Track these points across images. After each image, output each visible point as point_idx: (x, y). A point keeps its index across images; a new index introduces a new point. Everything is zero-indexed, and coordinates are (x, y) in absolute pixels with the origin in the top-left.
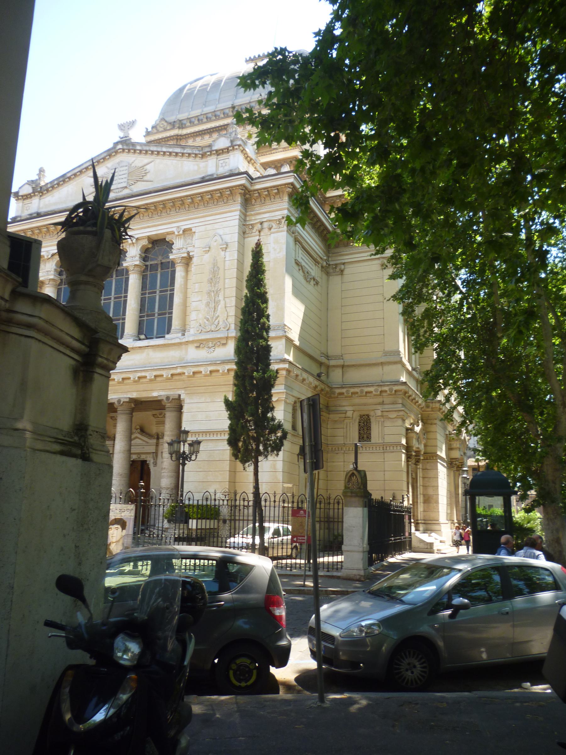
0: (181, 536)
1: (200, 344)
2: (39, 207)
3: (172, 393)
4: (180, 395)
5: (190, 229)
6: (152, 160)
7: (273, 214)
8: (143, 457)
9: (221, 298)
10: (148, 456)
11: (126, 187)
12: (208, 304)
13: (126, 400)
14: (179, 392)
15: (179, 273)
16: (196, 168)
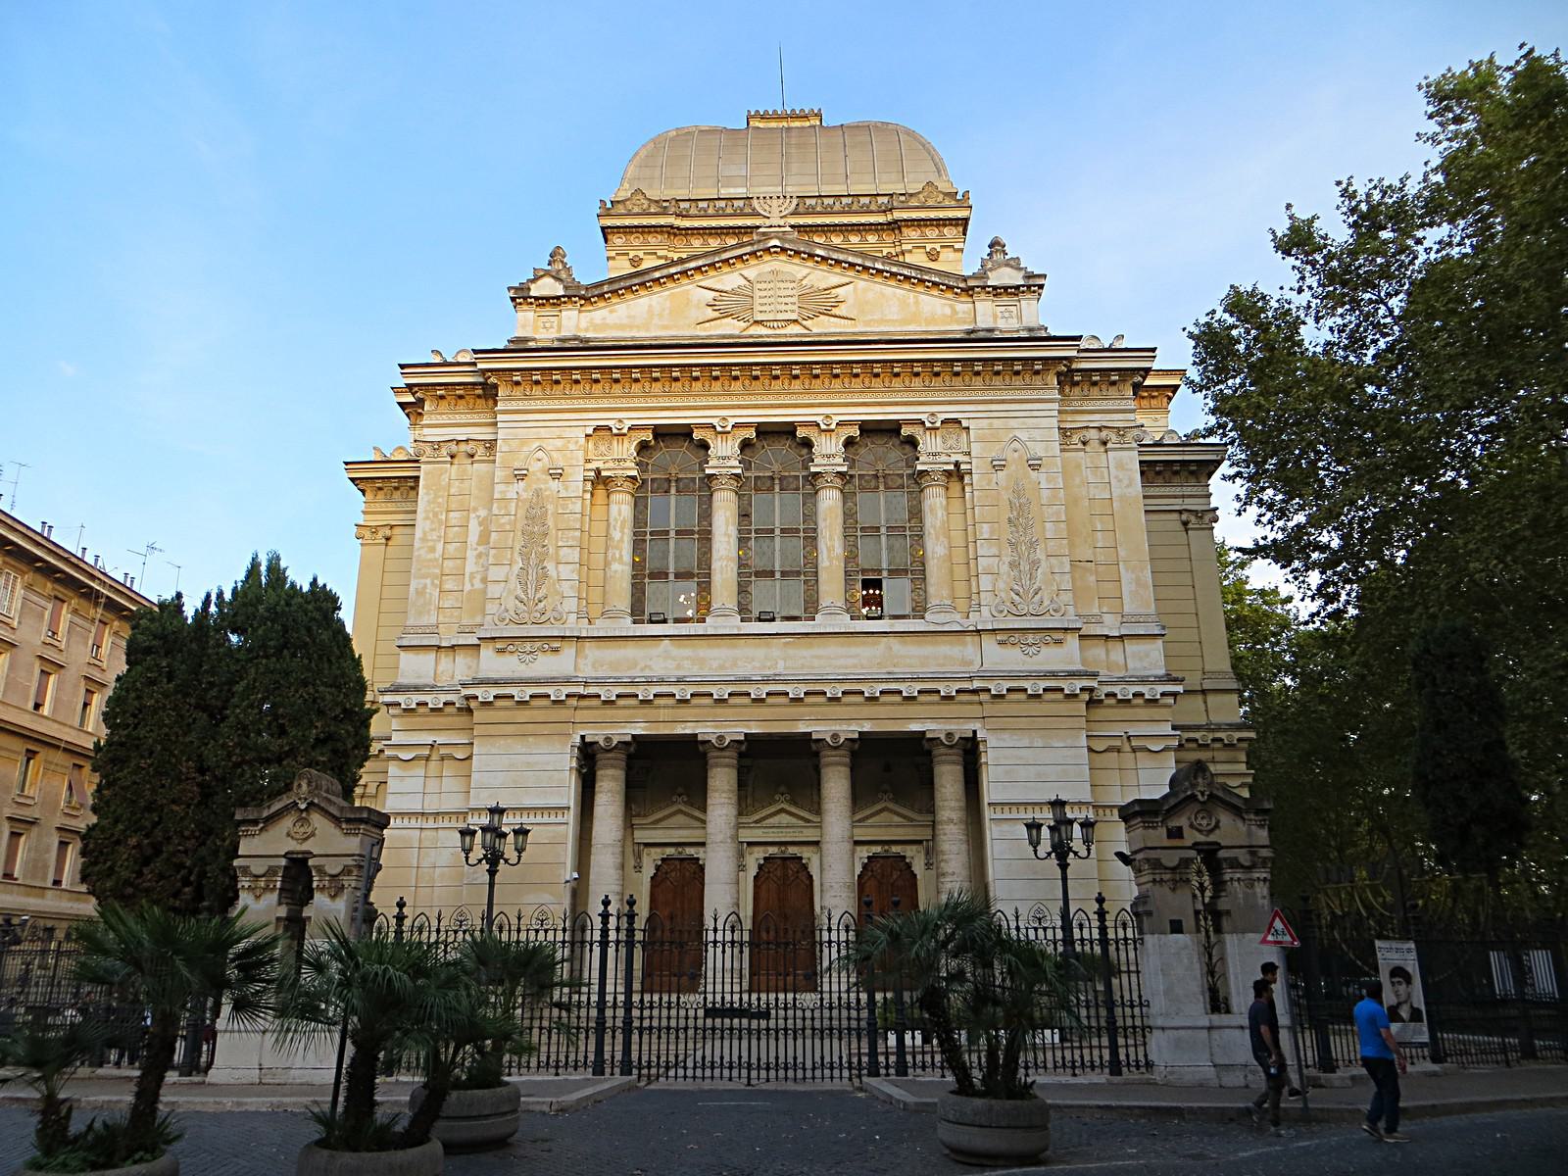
0: (736, 1006)
1: (1006, 635)
2: (577, 327)
3: (964, 728)
4: (975, 732)
5: (957, 421)
6: (847, 280)
7: (1108, 417)
8: (792, 850)
9: (1040, 554)
10: (908, 847)
11: (796, 321)
12: (1013, 565)
13: (850, 736)
14: (976, 725)
15: (935, 500)
16: (948, 311)
